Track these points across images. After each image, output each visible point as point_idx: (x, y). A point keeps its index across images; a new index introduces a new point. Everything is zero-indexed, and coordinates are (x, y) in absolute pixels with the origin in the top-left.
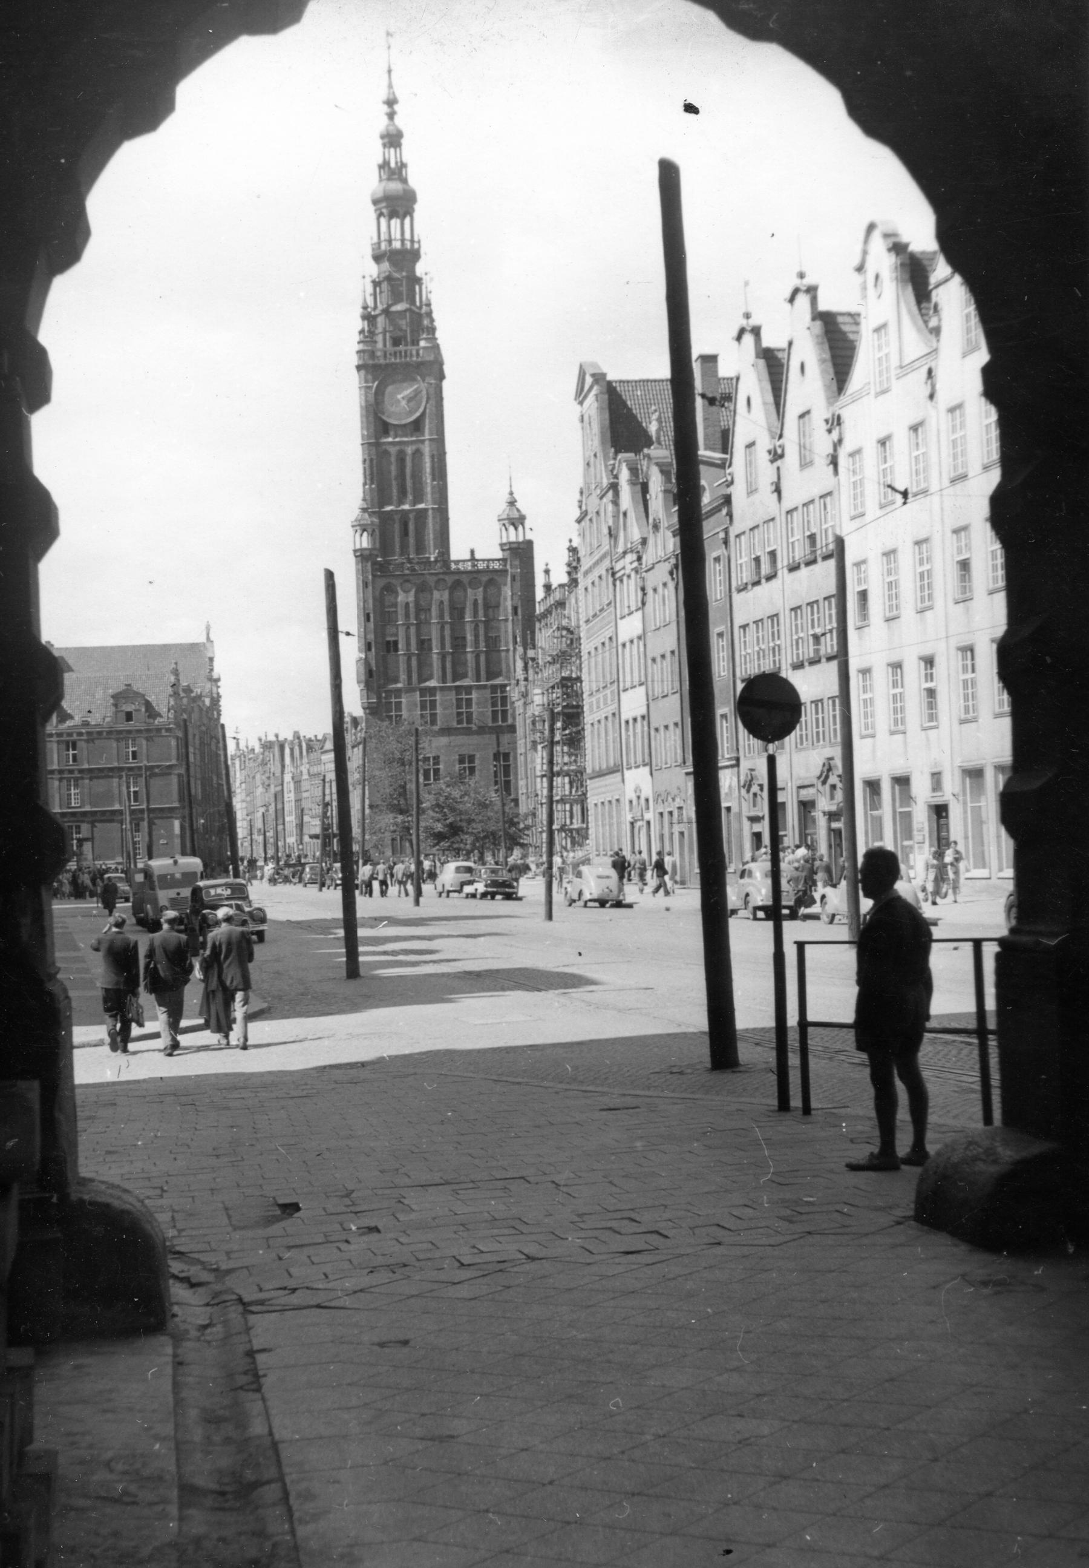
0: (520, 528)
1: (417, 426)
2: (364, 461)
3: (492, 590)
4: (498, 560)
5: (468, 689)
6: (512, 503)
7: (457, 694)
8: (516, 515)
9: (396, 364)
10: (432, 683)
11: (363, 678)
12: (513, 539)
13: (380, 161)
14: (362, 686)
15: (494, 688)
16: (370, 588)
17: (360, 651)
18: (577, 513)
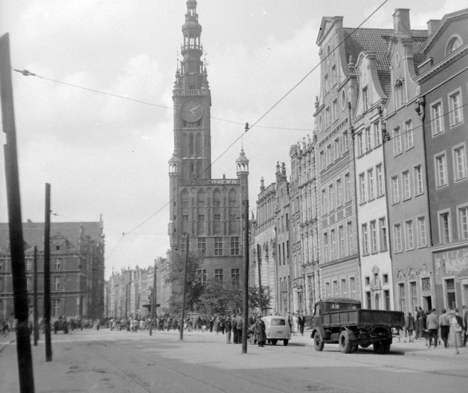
0: (246, 166)
1: (199, 123)
2: (175, 137)
3: (233, 194)
4: (236, 180)
5: (221, 238)
6: (243, 154)
7: (215, 241)
8: (244, 159)
9: (191, 96)
10: (204, 235)
11: (171, 232)
12: (243, 170)
13: (187, 13)
14: (171, 236)
15: (232, 238)
16: (176, 191)
17: (171, 220)
18: (314, 110)
